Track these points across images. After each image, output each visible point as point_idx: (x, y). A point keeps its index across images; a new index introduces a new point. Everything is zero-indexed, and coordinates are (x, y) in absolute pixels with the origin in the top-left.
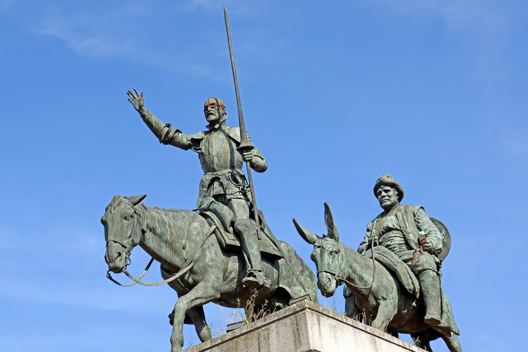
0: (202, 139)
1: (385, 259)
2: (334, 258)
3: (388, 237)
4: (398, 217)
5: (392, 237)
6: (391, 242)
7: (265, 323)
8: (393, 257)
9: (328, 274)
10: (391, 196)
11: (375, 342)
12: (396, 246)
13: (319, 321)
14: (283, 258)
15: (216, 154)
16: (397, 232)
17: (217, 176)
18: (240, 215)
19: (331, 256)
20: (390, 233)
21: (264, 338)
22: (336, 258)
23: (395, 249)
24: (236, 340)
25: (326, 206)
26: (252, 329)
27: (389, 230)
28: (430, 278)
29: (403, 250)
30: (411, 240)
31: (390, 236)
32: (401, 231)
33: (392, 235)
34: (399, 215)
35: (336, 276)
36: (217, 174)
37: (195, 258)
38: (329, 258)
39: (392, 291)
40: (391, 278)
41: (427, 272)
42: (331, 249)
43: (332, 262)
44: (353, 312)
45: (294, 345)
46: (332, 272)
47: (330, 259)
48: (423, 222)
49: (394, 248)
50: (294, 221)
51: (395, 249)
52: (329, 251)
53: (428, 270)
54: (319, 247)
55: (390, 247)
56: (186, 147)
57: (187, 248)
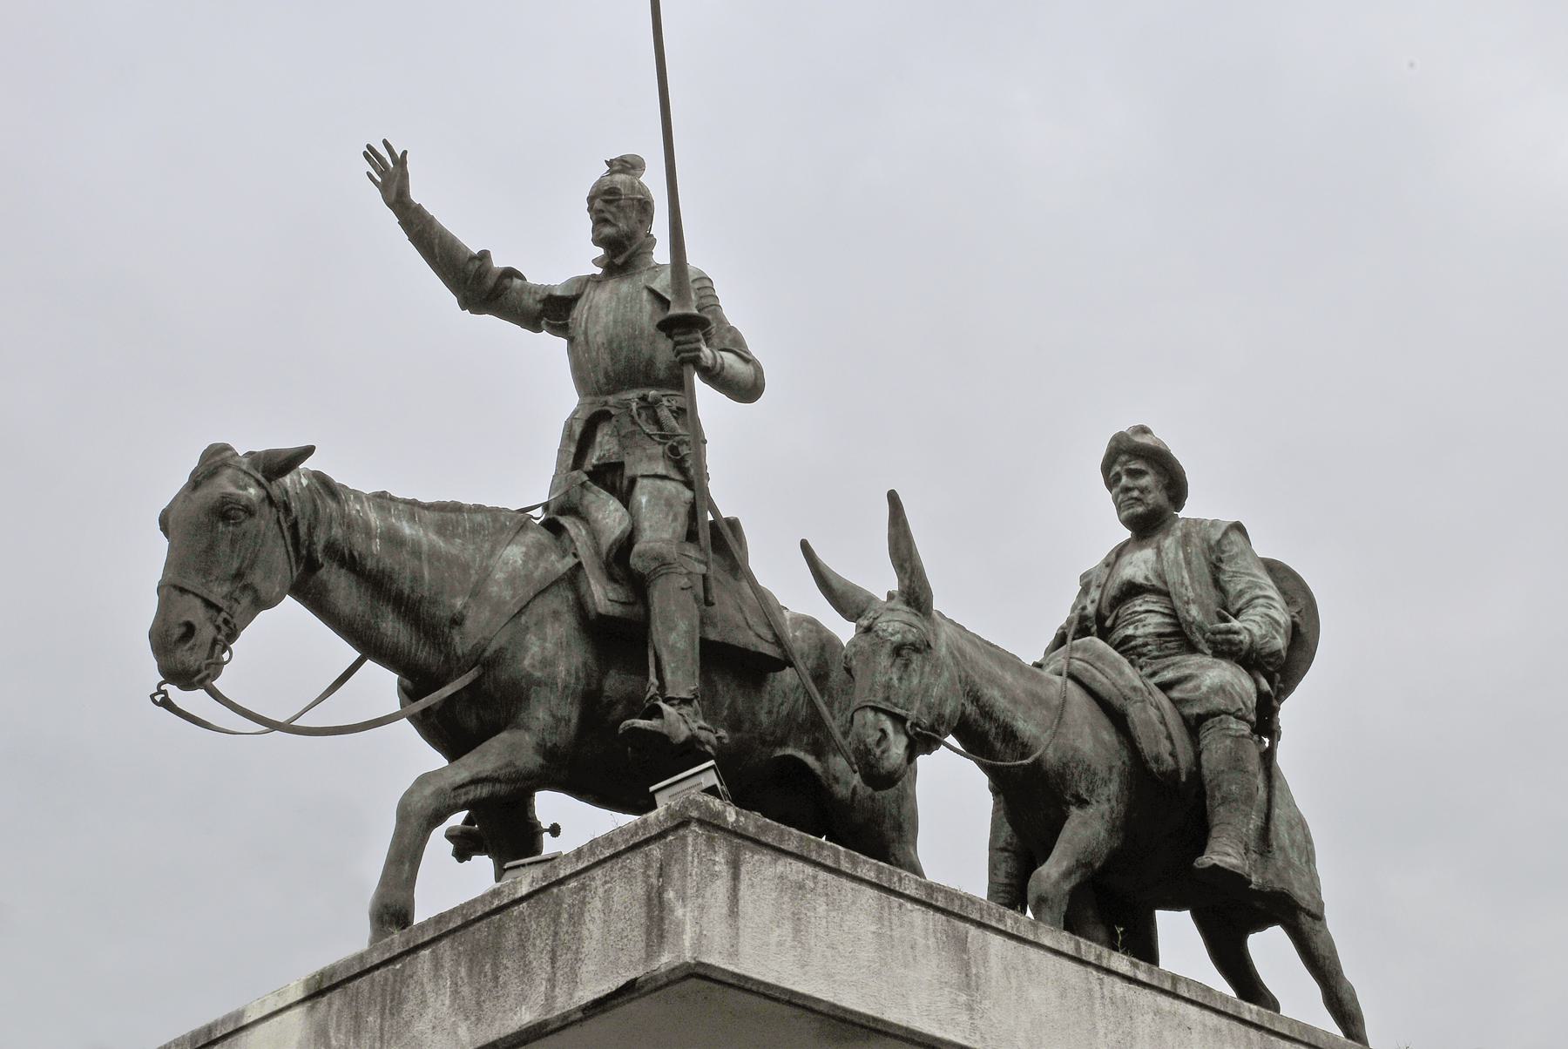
1: (1099, 676)
2: (906, 666)
3: (1131, 614)
4: (1163, 554)
5: (1141, 613)
6: (1136, 628)
7: (580, 866)
8: (1121, 673)
9: (883, 717)
10: (1146, 488)
11: (961, 944)
12: (1150, 640)
13: (735, 866)
14: (791, 665)
15: (605, 341)
16: (1154, 598)
17: (607, 408)
18: (651, 526)
19: (899, 662)
20: (1138, 602)
21: (571, 916)
22: (914, 665)
23: (1145, 650)
24: (500, 919)
25: (893, 498)
26: (544, 884)
28: (1228, 742)
29: (1168, 652)
30: (1193, 623)
32: (1167, 594)
33: (1141, 606)
34: (1166, 546)
35: (908, 724)
38: (892, 665)
39: (1107, 776)
42: (897, 638)
43: (900, 679)
45: (643, 944)
46: (898, 711)
47: (894, 670)
48: (1234, 569)
49: (1145, 645)
50: (805, 547)
51: (1145, 650)
53: (1223, 716)
55: (1133, 643)
56: (532, 321)
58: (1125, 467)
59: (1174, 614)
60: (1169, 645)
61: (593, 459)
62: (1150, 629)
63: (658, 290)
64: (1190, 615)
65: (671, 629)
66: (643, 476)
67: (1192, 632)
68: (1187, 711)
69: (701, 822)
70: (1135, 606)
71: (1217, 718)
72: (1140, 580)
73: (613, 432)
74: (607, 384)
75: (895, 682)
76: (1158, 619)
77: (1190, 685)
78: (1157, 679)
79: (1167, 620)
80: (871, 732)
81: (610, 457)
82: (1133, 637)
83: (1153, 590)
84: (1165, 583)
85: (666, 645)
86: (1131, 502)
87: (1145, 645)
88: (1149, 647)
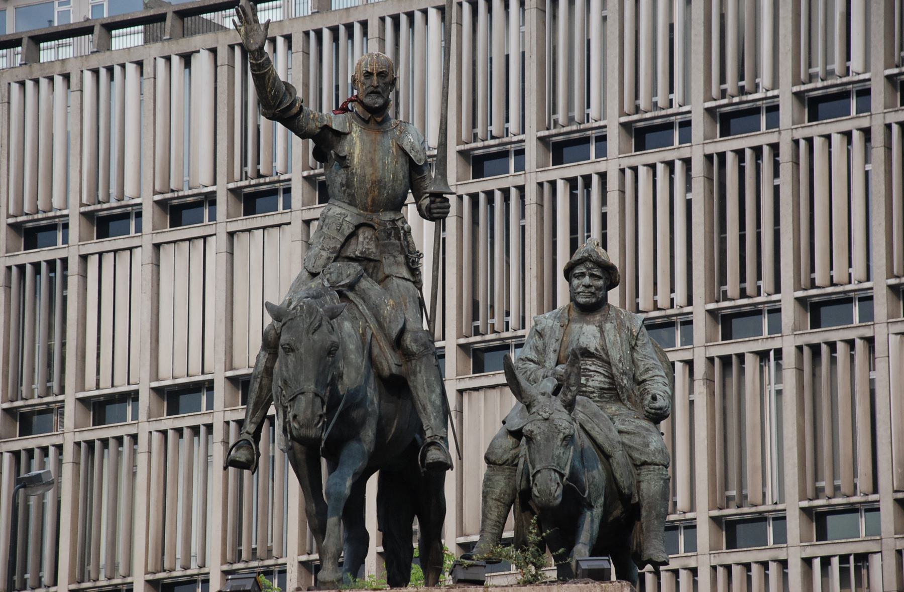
0: (346, 134)
4: (606, 334)
16: (600, 363)
29: (604, 400)
31: (588, 367)
32: (609, 363)
33: (591, 366)
41: (660, 468)
42: (567, 432)
43: (563, 453)
44: (502, 496)
48: (644, 353)
49: (593, 392)
52: (564, 433)
53: (661, 467)
55: (584, 389)
57: (345, 377)
58: (590, 271)
59: (610, 376)
60: (605, 395)
61: (355, 249)
62: (596, 384)
63: (407, 151)
64: (623, 382)
66: (396, 277)
67: (623, 393)
68: (636, 455)
70: (587, 365)
72: (592, 350)
73: (371, 237)
74: (372, 206)
75: (562, 454)
76: (602, 378)
77: (638, 440)
79: (607, 380)
80: (553, 484)
81: (369, 254)
83: (599, 358)
84: (607, 354)
85: (430, 401)
86: (589, 294)
88: (595, 395)
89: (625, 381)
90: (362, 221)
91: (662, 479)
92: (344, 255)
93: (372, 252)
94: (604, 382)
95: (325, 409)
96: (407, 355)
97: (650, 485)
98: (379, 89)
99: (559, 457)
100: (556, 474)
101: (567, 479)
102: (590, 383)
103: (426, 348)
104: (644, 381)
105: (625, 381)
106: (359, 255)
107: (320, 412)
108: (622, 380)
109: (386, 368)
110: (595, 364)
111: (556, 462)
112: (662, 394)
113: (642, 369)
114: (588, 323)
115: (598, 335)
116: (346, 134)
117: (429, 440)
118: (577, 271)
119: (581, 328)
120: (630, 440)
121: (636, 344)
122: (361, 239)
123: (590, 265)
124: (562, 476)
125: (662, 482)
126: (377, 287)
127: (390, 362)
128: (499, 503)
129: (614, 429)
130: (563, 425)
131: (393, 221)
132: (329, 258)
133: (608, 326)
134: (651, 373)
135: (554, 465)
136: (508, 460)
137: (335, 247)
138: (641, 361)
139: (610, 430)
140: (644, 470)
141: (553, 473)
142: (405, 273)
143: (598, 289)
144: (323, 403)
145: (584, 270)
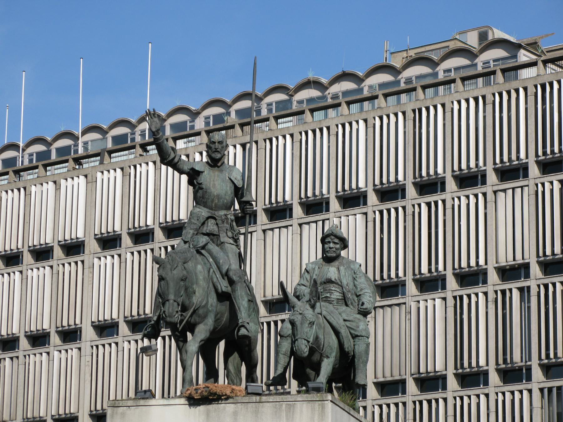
0: (202, 172)
1: (332, 319)
5: (332, 290)
6: (331, 295)
16: (337, 286)
17: (214, 216)
23: (333, 302)
27: (330, 281)
31: (331, 288)
36: (215, 214)
37: (203, 304)
40: (334, 337)
43: (309, 331)
49: (333, 301)
51: (333, 302)
53: (365, 337)
54: (300, 314)
55: (329, 299)
57: (197, 293)
65: (243, 300)
67: (348, 301)
68: (352, 332)
69: (331, 401)
70: (331, 287)
71: (363, 338)
72: (333, 280)
75: (308, 331)
76: (338, 294)
77: (354, 324)
78: (348, 324)
80: (304, 346)
81: (214, 231)
82: (330, 298)
83: (337, 284)
85: (242, 304)
87: (333, 301)
88: (334, 302)
89: (350, 295)
90: (210, 215)
91: (365, 344)
92: (201, 232)
93: (215, 231)
94: (339, 296)
95: (180, 308)
96: (231, 282)
97: (360, 347)
98: (218, 150)
99: (307, 333)
100: (305, 341)
101: (311, 343)
102: (332, 296)
103: (240, 278)
104: (360, 295)
105: (350, 295)
106: (208, 232)
107: (176, 310)
108: (348, 295)
109: (220, 288)
110: (335, 287)
111: (305, 335)
112: (368, 301)
113: (359, 289)
114: (332, 266)
115: (337, 272)
116: (202, 172)
117: (240, 324)
118: (326, 240)
119: (329, 269)
120: (350, 324)
121: (356, 277)
122: (209, 224)
123: (333, 237)
124: (308, 342)
125: (365, 345)
126: (217, 248)
127: (224, 286)
128: (285, 356)
129: (341, 319)
130: (309, 316)
131: (226, 215)
132: (193, 234)
133: (342, 268)
134: (363, 291)
135: (305, 337)
136: (289, 335)
137: (197, 228)
138: (359, 285)
139: (339, 319)
140: (356, 340)
141: (303, 340)
142: (231, 241)
143: (337, 249)
144: (178, 305)
145: (330, 240)
